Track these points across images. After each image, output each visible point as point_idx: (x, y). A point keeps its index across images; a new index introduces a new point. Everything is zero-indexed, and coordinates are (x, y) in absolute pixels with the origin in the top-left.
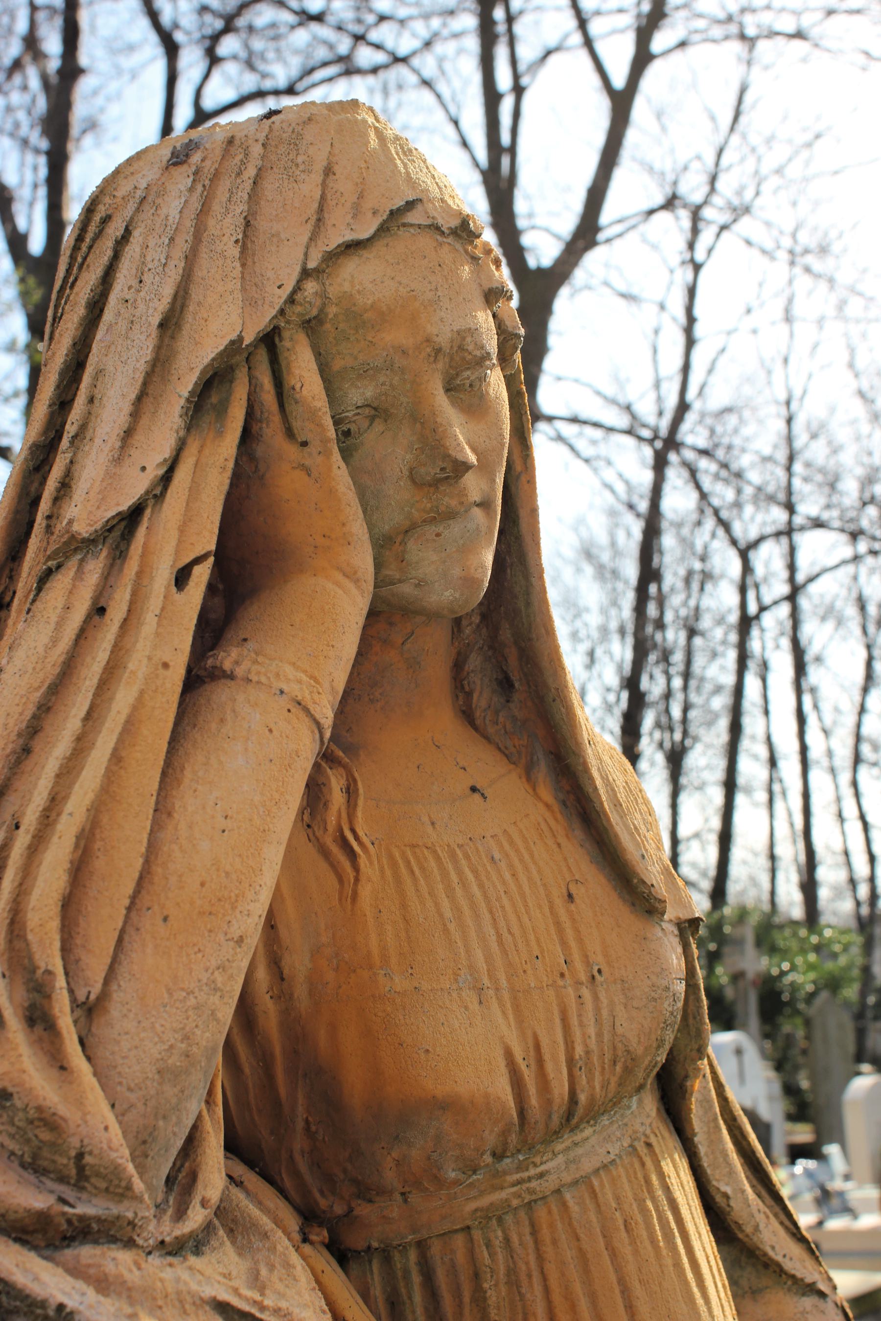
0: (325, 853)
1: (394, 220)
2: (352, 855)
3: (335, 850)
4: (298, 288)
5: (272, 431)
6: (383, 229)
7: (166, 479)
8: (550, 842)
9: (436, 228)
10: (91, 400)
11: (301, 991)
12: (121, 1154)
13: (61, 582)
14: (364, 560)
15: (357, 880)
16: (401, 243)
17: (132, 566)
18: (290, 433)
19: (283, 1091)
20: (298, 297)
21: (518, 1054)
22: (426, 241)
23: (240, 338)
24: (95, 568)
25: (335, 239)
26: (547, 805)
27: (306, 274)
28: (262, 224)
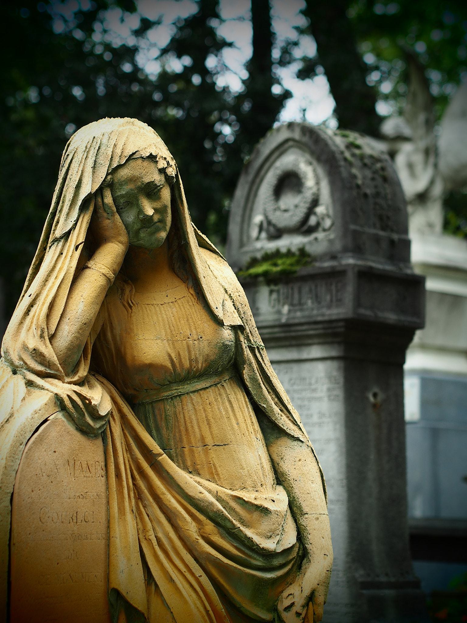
0: (124, 306)
1: (131, 158)
2: (131, 307)
3: (127, 305)
4: (106, 177)
5: (101, 211)
6: (127, 161)
7: (76, 224)
8: (191, 304)
9: (142, 158)
10: (63, 202)
11: (118, 338)
12: (57, 362)
13: (53, 248)
14: (124, 238)
15: (132, 312)
16: (132, 163)
17: (68, 244)
18: (105, 210)
19: (115, 363)
20: (106, 180)
21: (173, 356)
22: (140, 162)
23: (91, 193)
24: (61, 244)
25: (115, 165)
26: (192, 295)
27: (108, 174)
28: (99, 161)
